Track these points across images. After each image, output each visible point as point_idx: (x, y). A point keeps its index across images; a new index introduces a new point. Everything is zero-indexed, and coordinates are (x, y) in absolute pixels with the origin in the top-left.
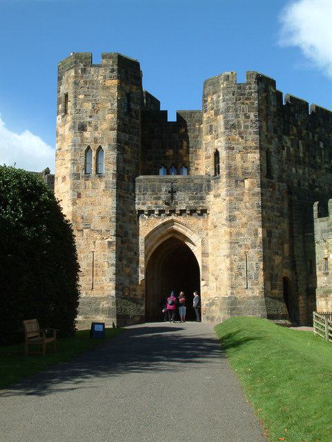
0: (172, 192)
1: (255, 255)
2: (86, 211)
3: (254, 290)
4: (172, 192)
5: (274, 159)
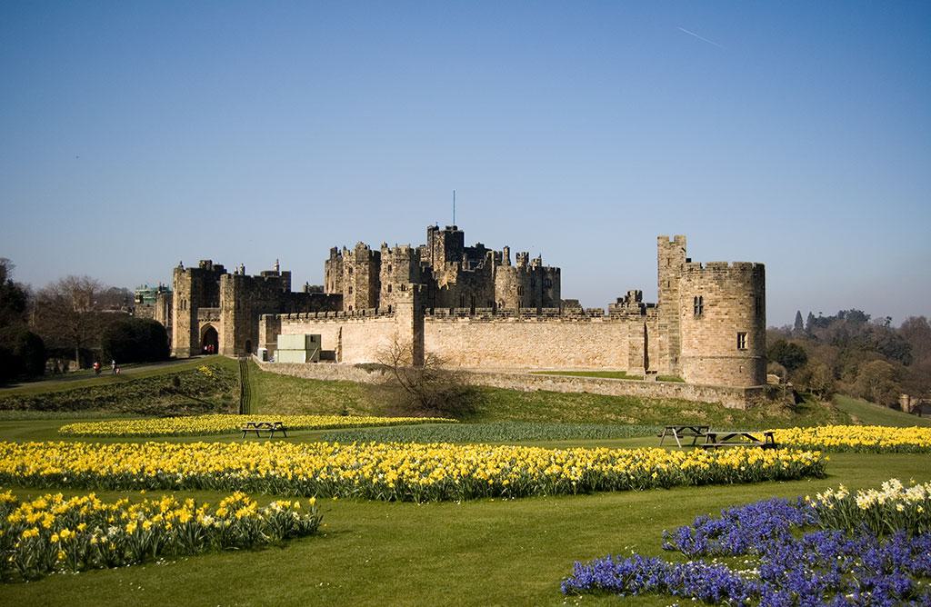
0: (209, 314)
1: (232, 335)
2: (181, 321)
3: (231, 346)
4: (209, 314)
5: (241, 305)
